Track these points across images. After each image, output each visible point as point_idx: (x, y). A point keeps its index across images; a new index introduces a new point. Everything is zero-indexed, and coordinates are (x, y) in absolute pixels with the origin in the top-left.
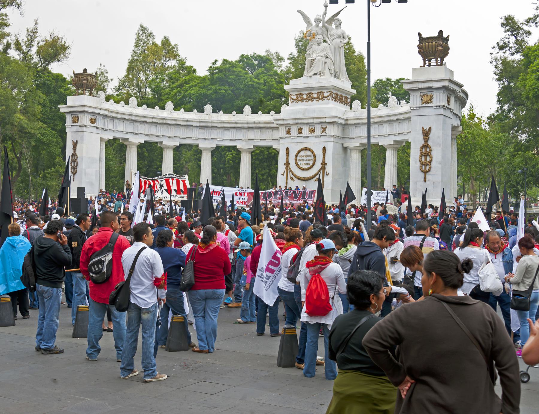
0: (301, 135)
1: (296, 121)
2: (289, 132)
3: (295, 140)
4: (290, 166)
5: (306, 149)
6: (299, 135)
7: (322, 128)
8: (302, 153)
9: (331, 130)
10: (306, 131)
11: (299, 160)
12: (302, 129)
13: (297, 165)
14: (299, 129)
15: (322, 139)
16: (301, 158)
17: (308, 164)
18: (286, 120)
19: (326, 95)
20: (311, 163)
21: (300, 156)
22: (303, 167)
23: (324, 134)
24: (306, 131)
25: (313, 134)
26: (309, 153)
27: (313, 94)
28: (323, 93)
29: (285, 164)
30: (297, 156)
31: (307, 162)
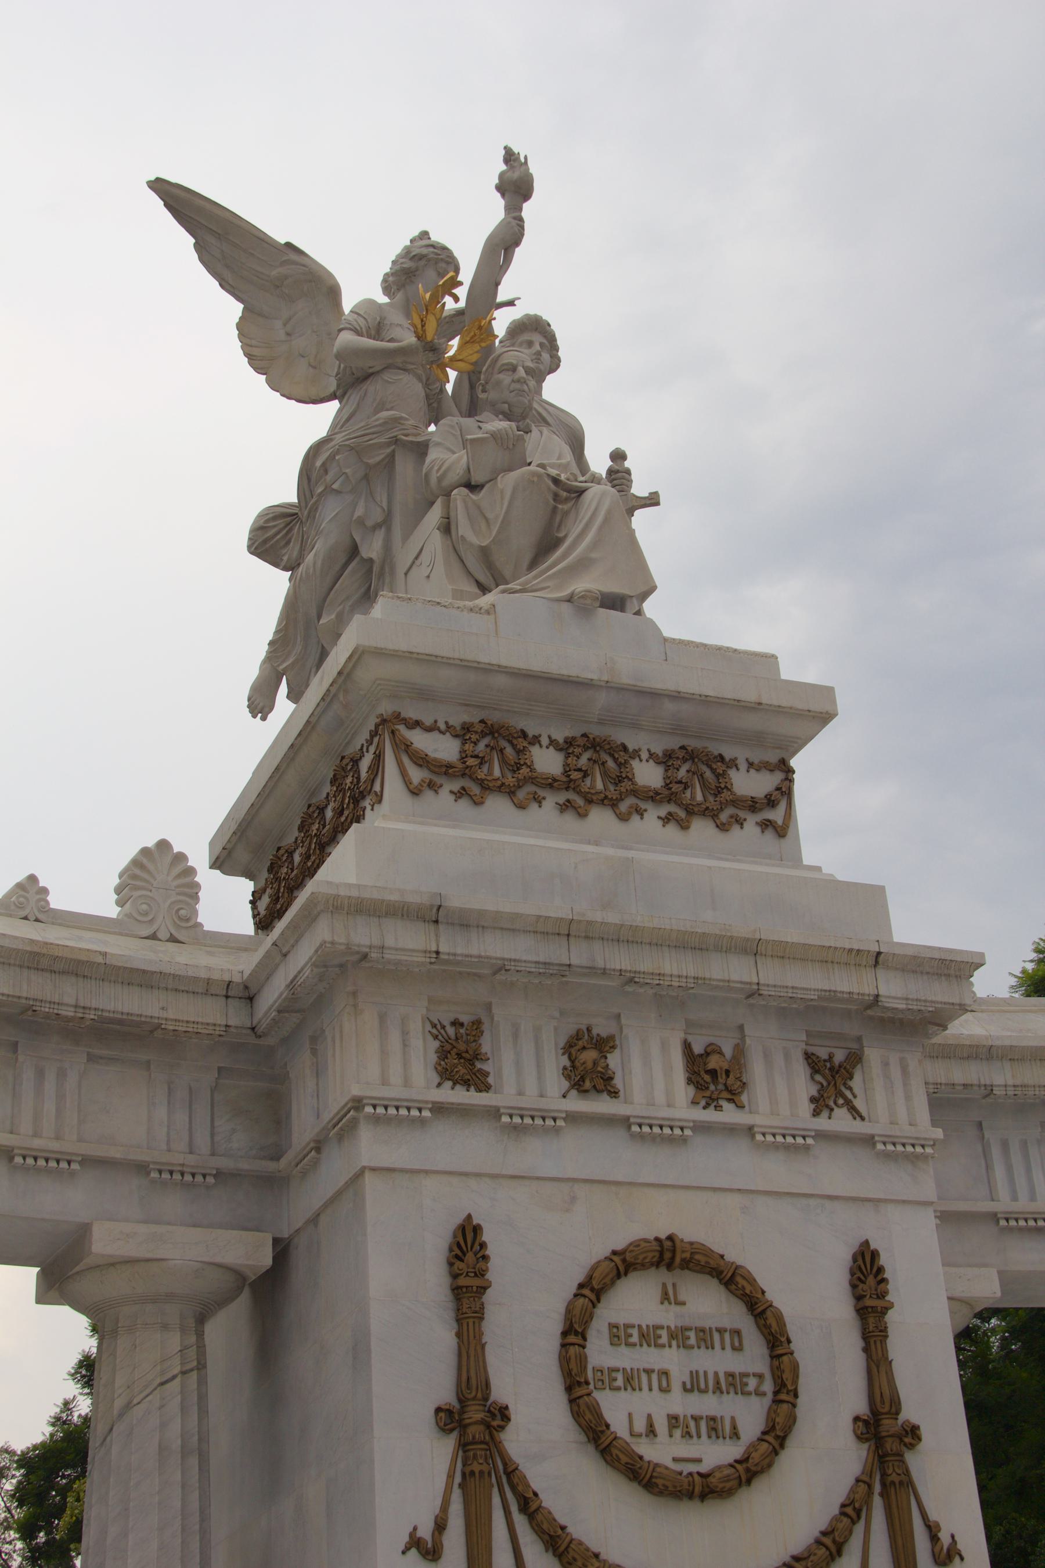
0: (602, 1105)
1: (578, 955)
2: (462, 1058)
3: (536, 1155)
4: (516, 1441)
5: (668, 1256)
6: (577, 1104)
7: (813, 1063)
8: (635, 1301)
9: (893, 1094)
10: (652, 1075)
11: (607, 1377)
12: (604, 1045)
13: (594, 1432)
14: (572, 1046)
15: (834, 1172)
16: (625, 1358)
17: (714, 1427)
18: (467, 922)
19: (748, 784)
20: (750, 1415)
21: (618, 1335)
22: (662, 1452)
23: (840, 1121)
24: (652, 1075)
25: (728, 1114)
26: (706, 1304)
27: (623, 754)
28: (721, 765)
29: (448, 1419)
30: (574, 1332)
31: (708, 1405)
